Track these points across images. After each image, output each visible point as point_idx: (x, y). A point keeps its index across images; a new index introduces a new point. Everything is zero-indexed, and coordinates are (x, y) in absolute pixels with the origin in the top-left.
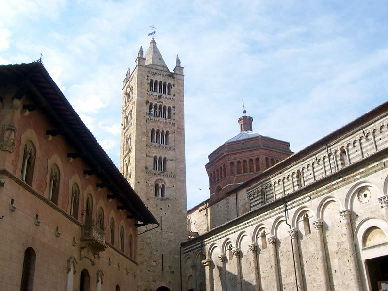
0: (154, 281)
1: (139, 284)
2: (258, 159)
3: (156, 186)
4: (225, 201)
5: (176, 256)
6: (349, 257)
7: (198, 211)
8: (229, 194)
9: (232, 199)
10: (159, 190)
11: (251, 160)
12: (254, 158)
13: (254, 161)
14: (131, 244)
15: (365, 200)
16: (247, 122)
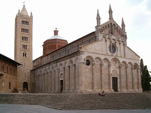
0: (23, 80)
1: (19, 81)
2: (55, 45)
3: (24, 54)
4: (45, 57)
5: (29, 74)
6: (58, 79)
7: (40, 59)
8: (46, 55)
9: (47, 57)
10: (25, 55)
11: (54, 46)
12: (54, 45)
13: (53, 46)
14: (14, 71)
15: (62, 67)
16: (56, 33)
